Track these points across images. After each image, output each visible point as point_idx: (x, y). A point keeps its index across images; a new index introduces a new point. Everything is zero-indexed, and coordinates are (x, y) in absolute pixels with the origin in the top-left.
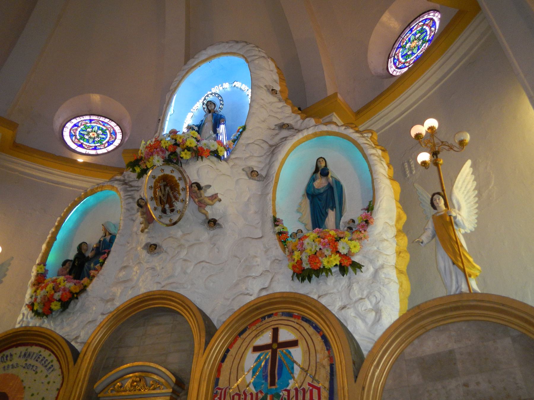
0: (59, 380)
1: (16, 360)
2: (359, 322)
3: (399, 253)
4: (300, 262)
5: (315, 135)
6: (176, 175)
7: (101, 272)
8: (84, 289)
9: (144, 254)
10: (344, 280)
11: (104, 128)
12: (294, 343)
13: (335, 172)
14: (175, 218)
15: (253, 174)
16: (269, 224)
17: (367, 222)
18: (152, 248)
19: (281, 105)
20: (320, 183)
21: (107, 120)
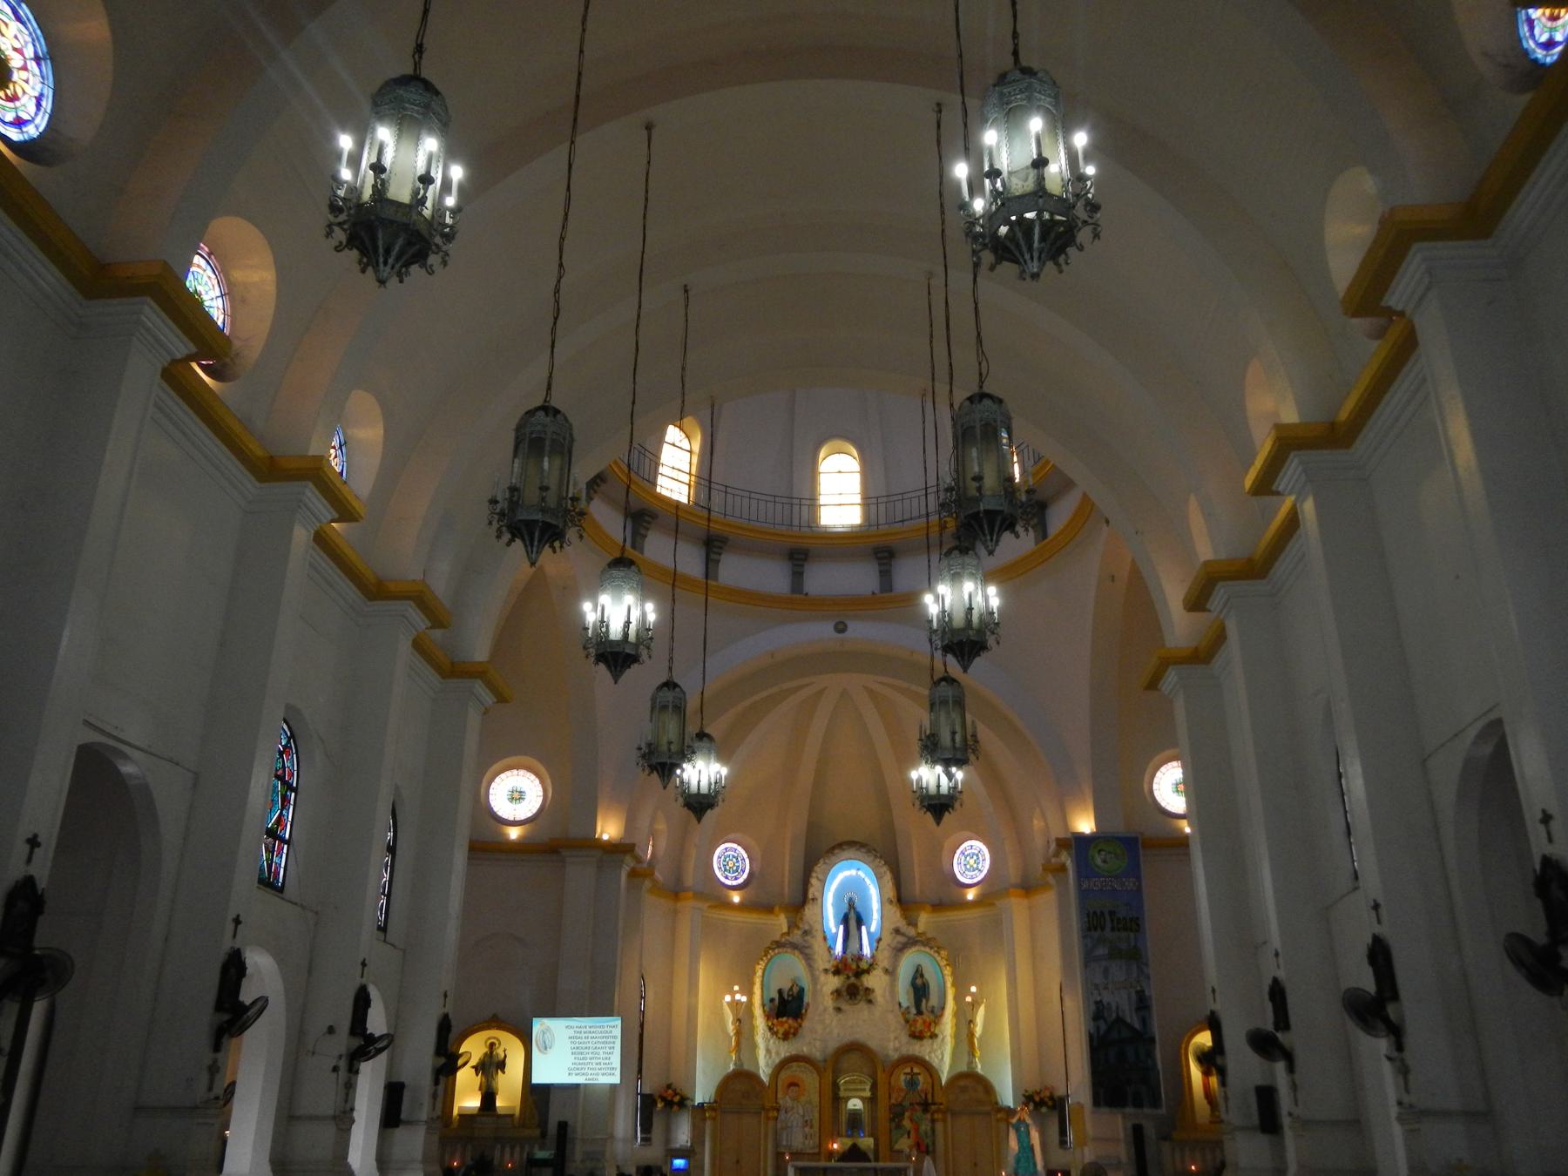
0: (818, 1078)
1: (794, 1069)
2: (936, 1060)
3: (952, 1028)
4: (914, 1032)
5: (918, 951)
6: (859, 984)
7: (808, 1016)
8: (800, 1026)
9: (831, 1010)
10: (930, 1041)
11: (736, 855)
12: (919, 1074)
13: (927, 976)
14: (856, 1002)
15: (886, 971)
16: (897, 1006)
17: (942, 1015)
18: (838, 1010)
19: (895, 909)
20: (919, 981)
21: (735, 846)
